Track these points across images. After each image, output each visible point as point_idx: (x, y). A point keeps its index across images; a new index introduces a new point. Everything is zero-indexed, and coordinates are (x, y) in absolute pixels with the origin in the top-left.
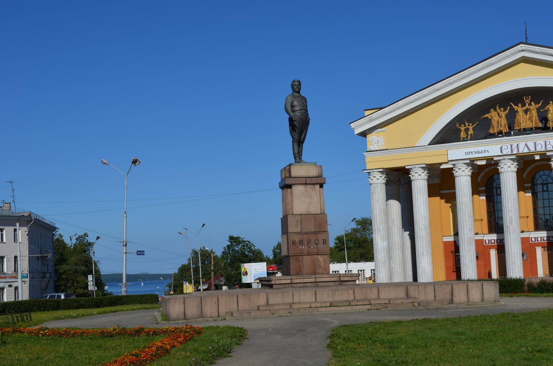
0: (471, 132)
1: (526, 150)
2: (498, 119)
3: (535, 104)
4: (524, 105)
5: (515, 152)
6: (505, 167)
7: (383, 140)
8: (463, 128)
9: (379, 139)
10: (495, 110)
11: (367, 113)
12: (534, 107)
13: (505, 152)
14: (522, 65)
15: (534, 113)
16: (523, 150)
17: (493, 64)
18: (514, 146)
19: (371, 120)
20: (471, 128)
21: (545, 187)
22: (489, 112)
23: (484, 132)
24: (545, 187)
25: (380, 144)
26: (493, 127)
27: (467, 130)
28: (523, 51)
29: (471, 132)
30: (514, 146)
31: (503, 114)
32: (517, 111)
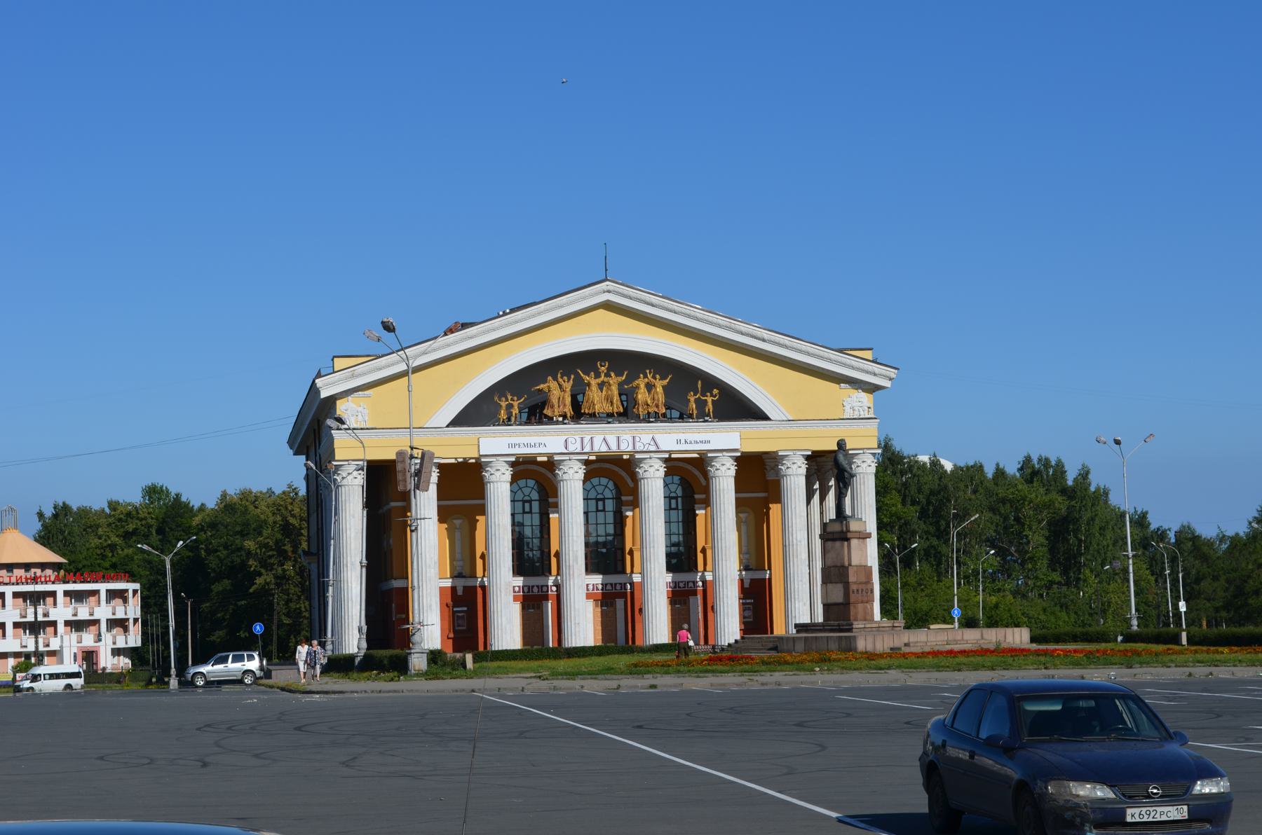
0: (515, 411)
1: (604, 449)
2: (558, 391)
3: (617, 375)
4: (598, 375)
5: (587, 449)
6: (571, 472)
7: (366, 411)
8: (504, 404)
9: (360, 409)
10: (555, 379)
11: (339, 364)
12: (614, 380)
13: (571, 449)
14: (601, 311)
15: (615, 390)
16: (599, 447)
17: (562, 307)
18: (587, 439)
19: (353, 376)
20: (516, 404)
21: (527, 505)
22: (545, 381)
23: (536, 414)
24: (527, 505)
25: (360, 418)
26: (552, 407)
27: (510, 406)
28: (609, 292)
29: (515, 411)
30: (587, 439)
31: (568, 386)
32: (589, 384)
